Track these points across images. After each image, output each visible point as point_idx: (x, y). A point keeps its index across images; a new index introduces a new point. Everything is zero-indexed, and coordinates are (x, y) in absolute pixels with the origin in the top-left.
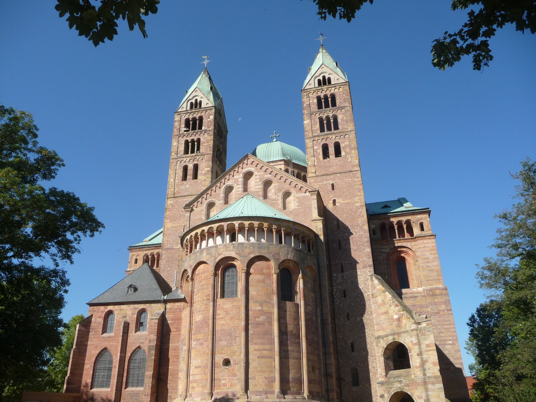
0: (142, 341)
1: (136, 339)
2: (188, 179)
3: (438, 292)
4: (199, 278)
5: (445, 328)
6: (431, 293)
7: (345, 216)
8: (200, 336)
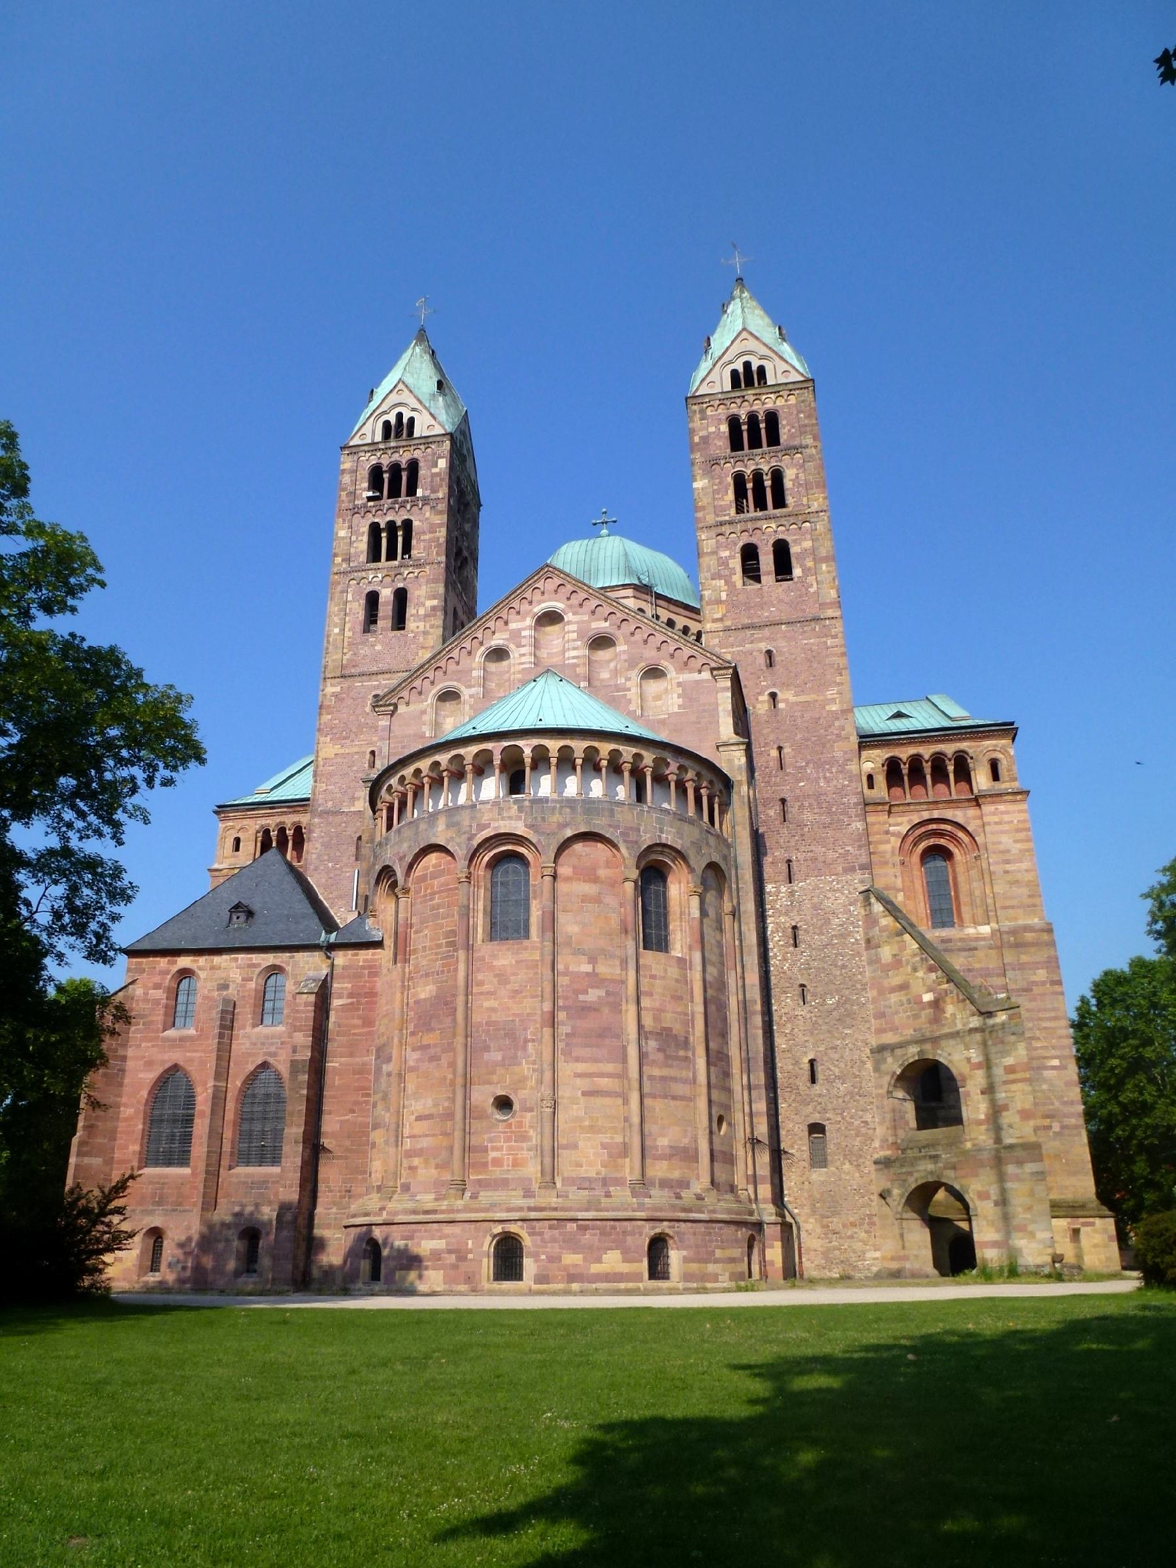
0: (273, 1049)
1: (255, 1044)
3: (1029, 936)
4: (426, 889)
5: (1045, 1028)
6: (1012, 939)
7: (799, 736)
8: (428, 1039)
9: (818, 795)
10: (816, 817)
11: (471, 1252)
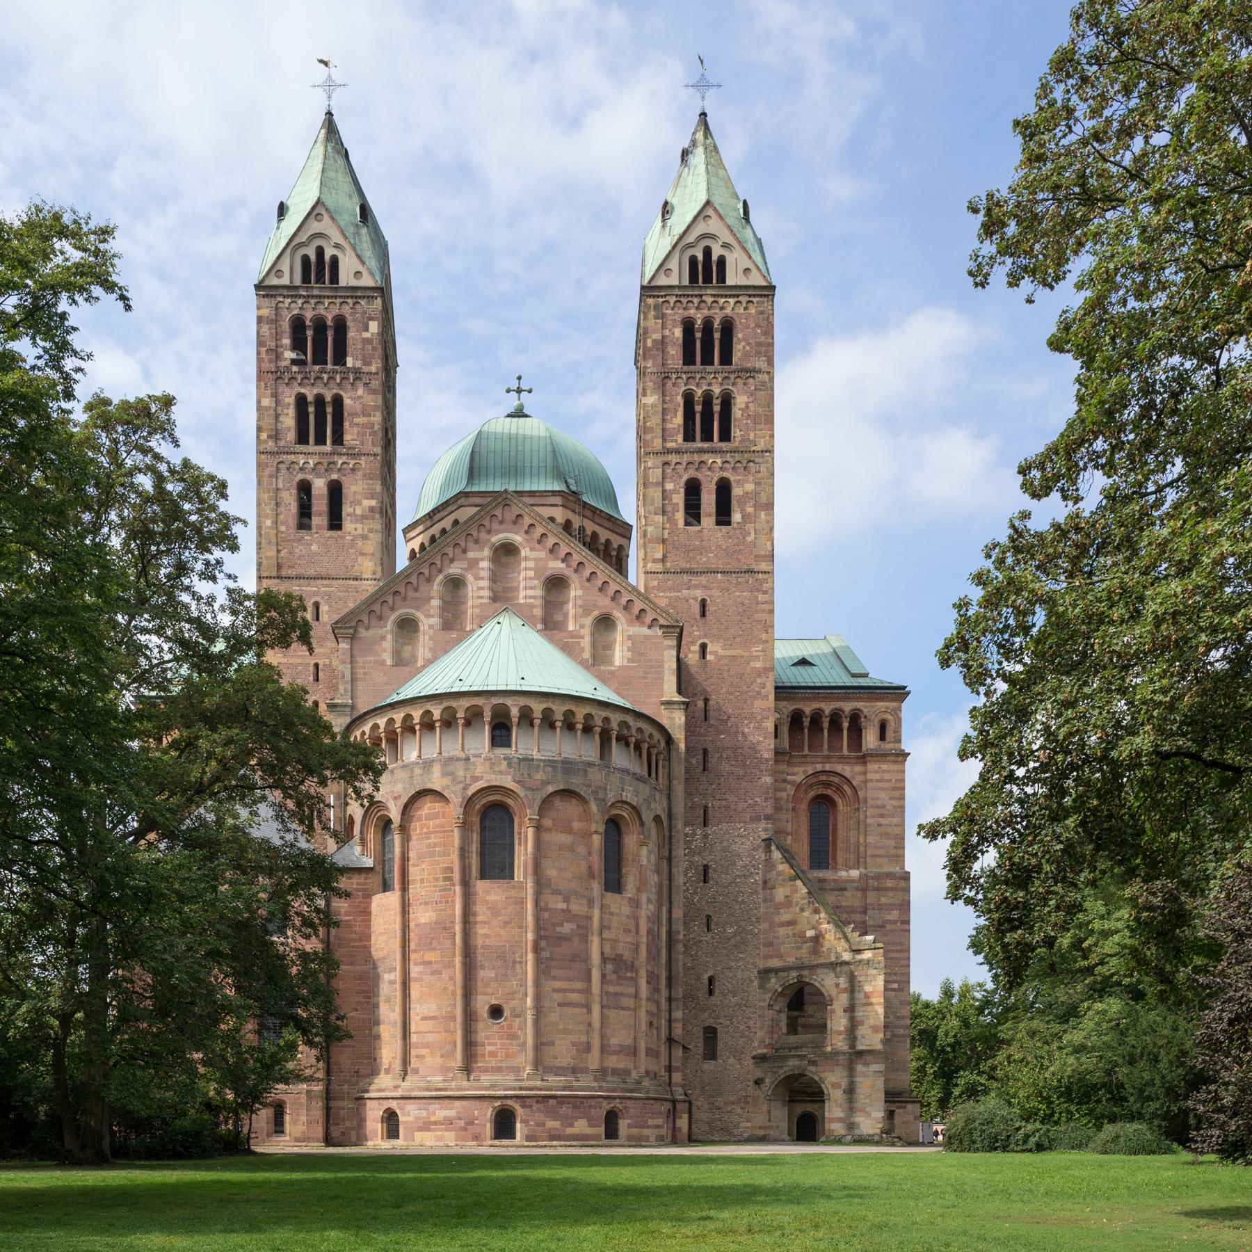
2: (314, 526)
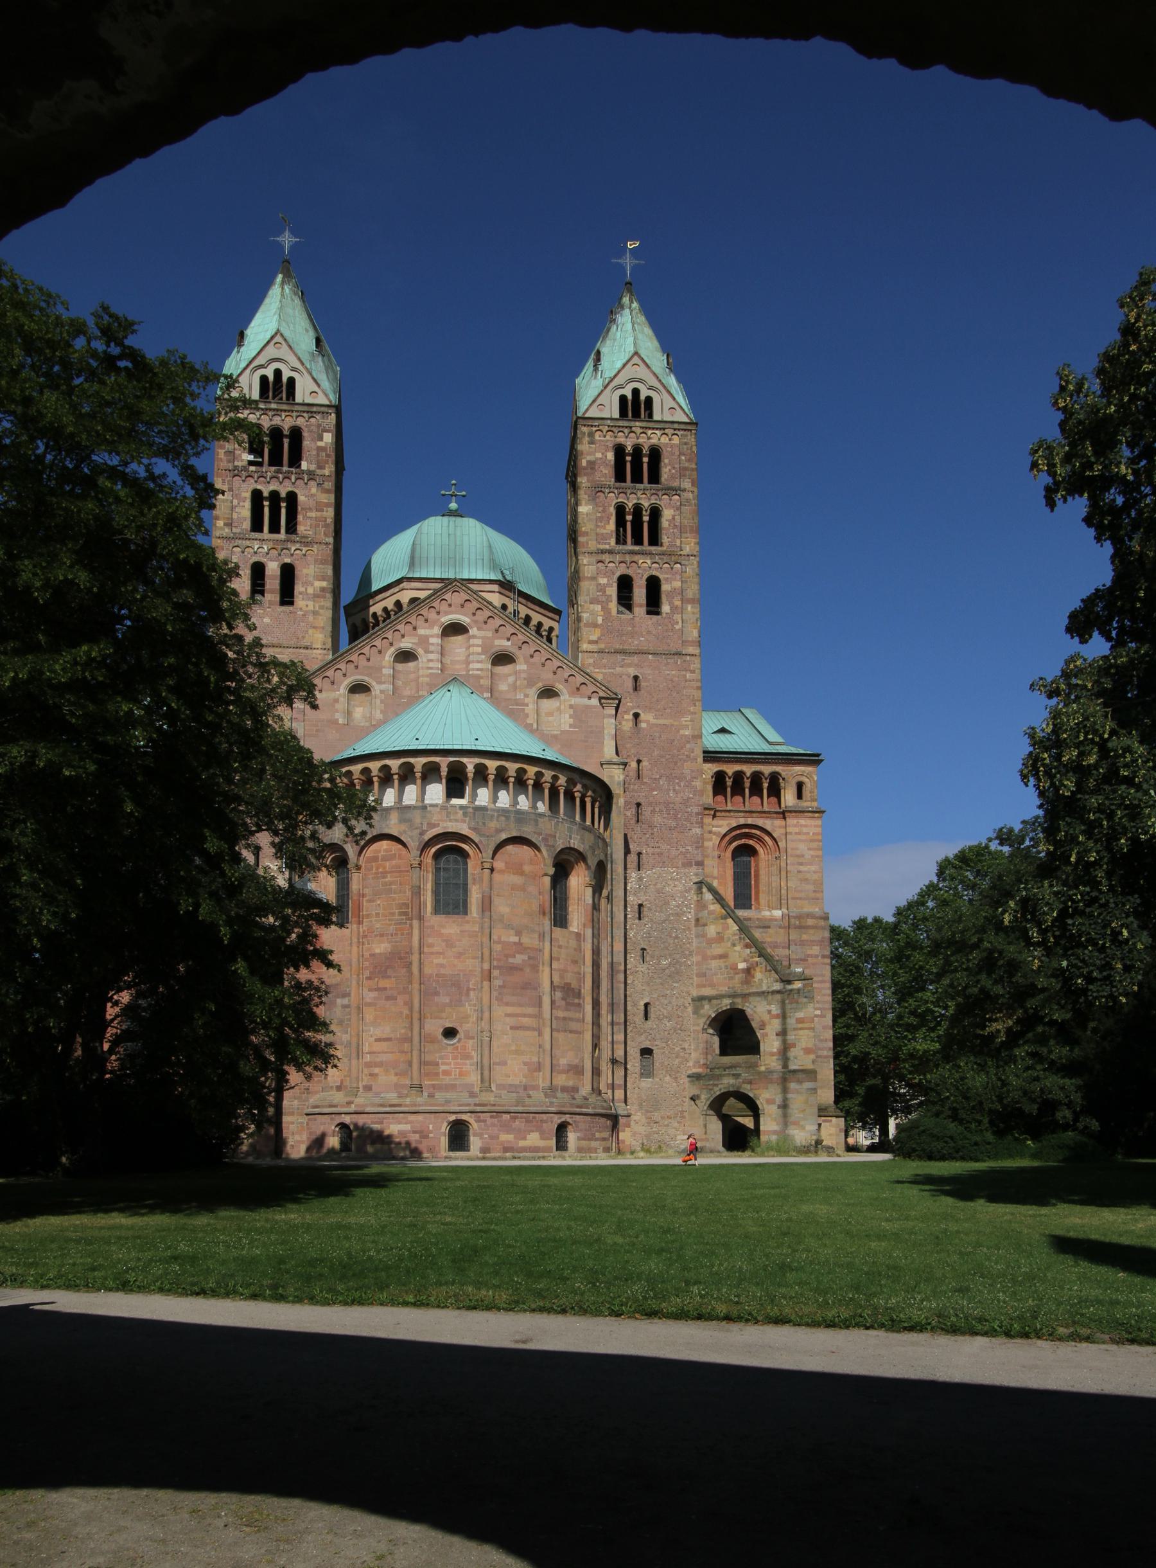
9: (667, 804)
10: (665, 820)
11: (431, 1132)
